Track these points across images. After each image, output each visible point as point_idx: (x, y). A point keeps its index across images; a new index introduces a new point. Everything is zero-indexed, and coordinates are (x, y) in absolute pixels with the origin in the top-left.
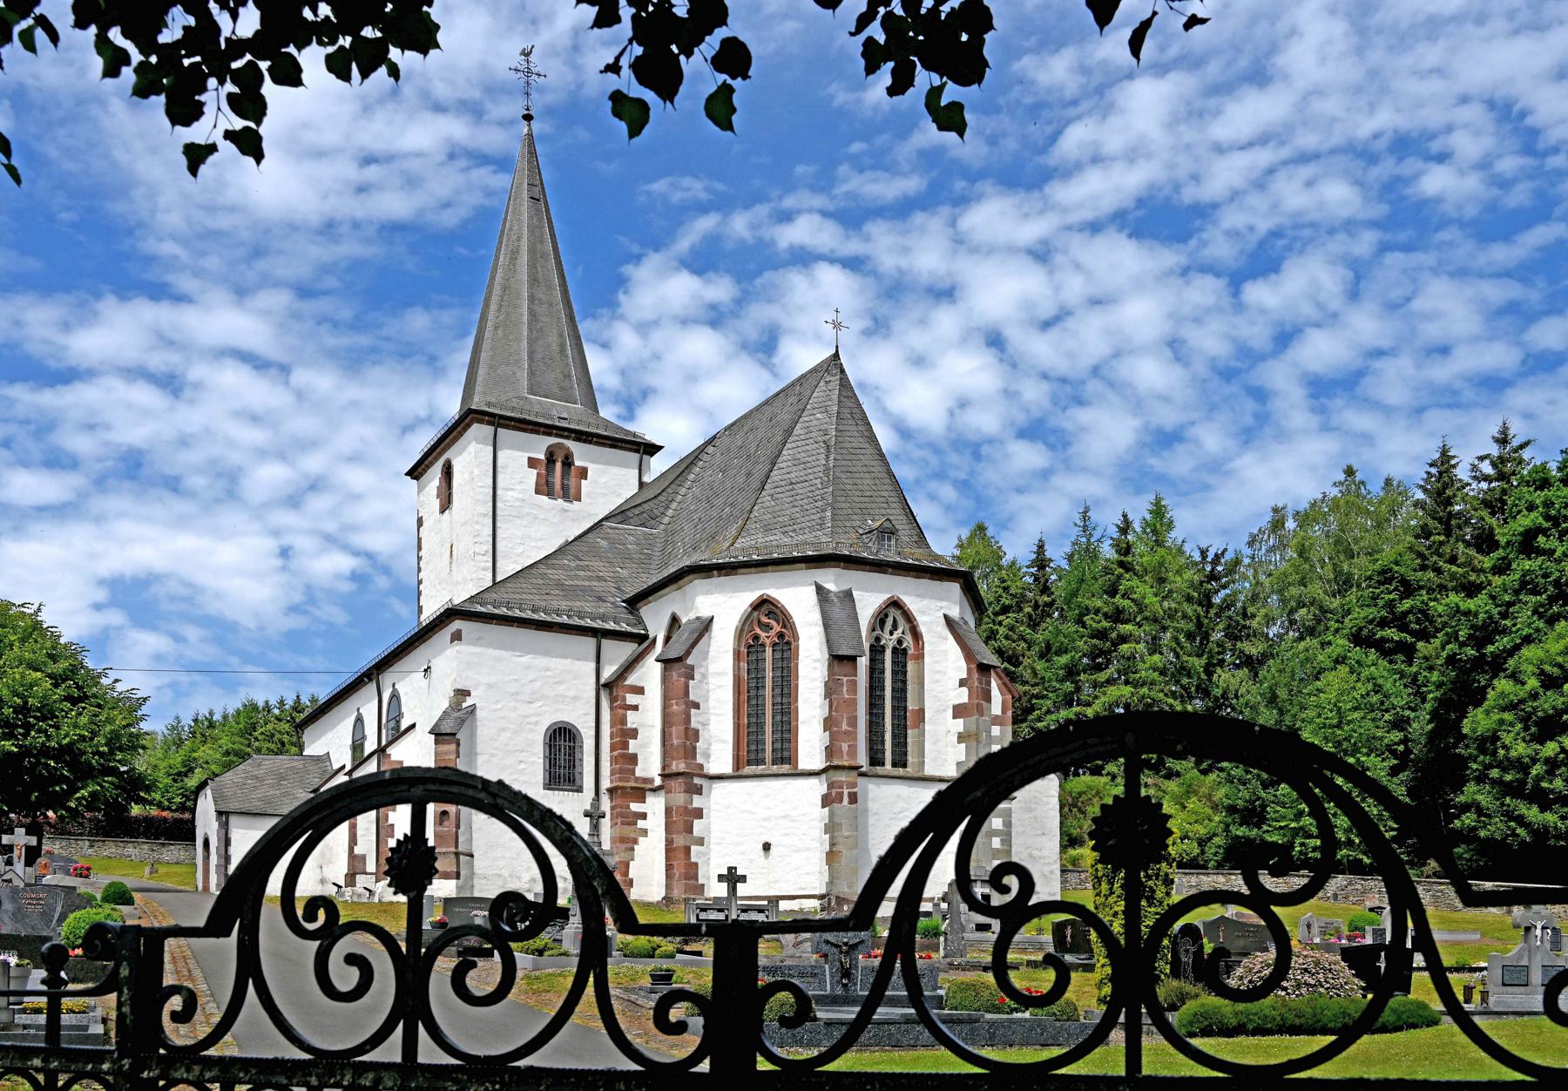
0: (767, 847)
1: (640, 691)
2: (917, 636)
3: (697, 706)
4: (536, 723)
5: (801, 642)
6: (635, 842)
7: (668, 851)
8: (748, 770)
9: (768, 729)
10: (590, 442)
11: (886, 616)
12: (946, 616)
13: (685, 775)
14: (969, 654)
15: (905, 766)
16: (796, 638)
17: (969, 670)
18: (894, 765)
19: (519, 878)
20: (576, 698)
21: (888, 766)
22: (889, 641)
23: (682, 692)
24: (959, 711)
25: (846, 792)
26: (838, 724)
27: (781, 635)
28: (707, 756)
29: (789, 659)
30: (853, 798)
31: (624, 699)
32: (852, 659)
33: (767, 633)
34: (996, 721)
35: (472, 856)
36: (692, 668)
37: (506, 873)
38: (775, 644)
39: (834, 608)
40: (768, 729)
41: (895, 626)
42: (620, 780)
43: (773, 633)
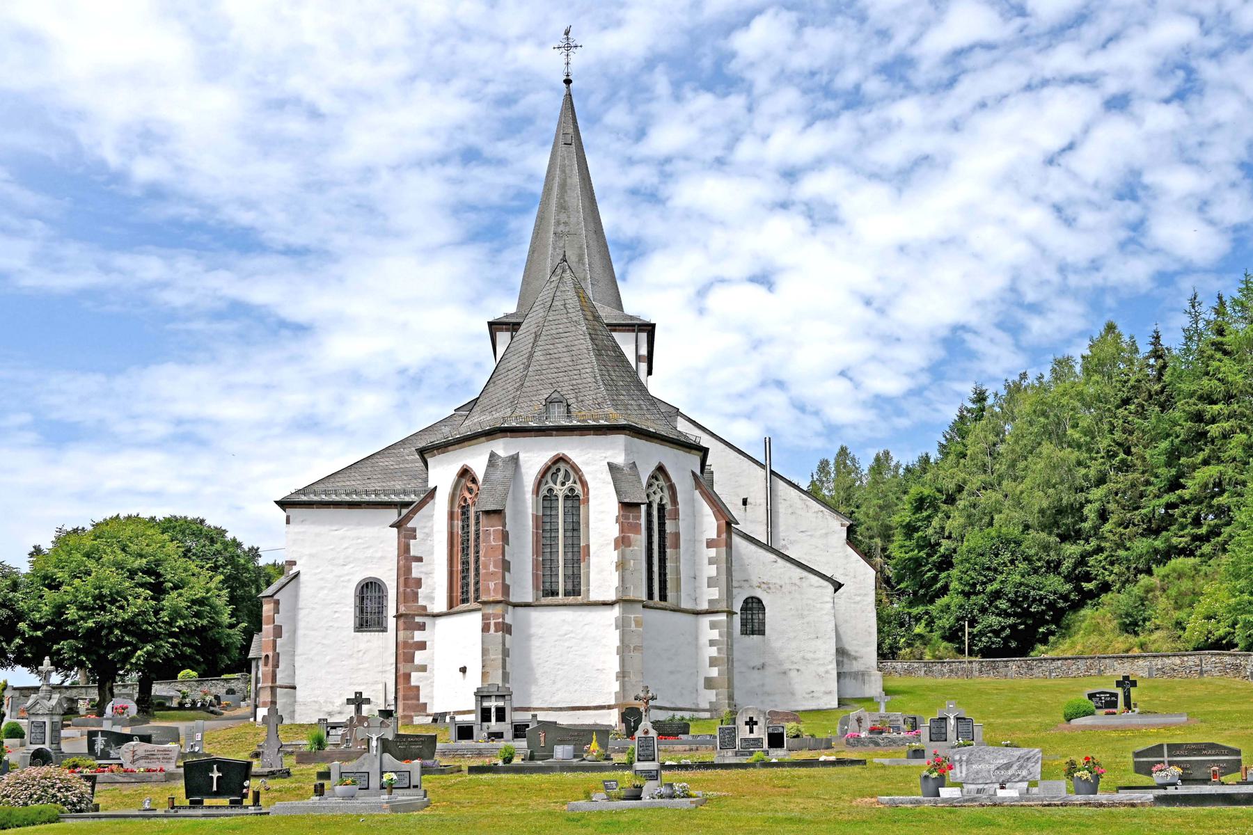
2: (584, 484)
3: (420, 559)
4: (349, 581)
11: (558, 470)
18: (566, 594)
19: (332, 703)
20: (382, 558)
22: (560, 491)
34: (710, 544)
35: (294, 688)
36: (414, 530)
37: (321, 700)
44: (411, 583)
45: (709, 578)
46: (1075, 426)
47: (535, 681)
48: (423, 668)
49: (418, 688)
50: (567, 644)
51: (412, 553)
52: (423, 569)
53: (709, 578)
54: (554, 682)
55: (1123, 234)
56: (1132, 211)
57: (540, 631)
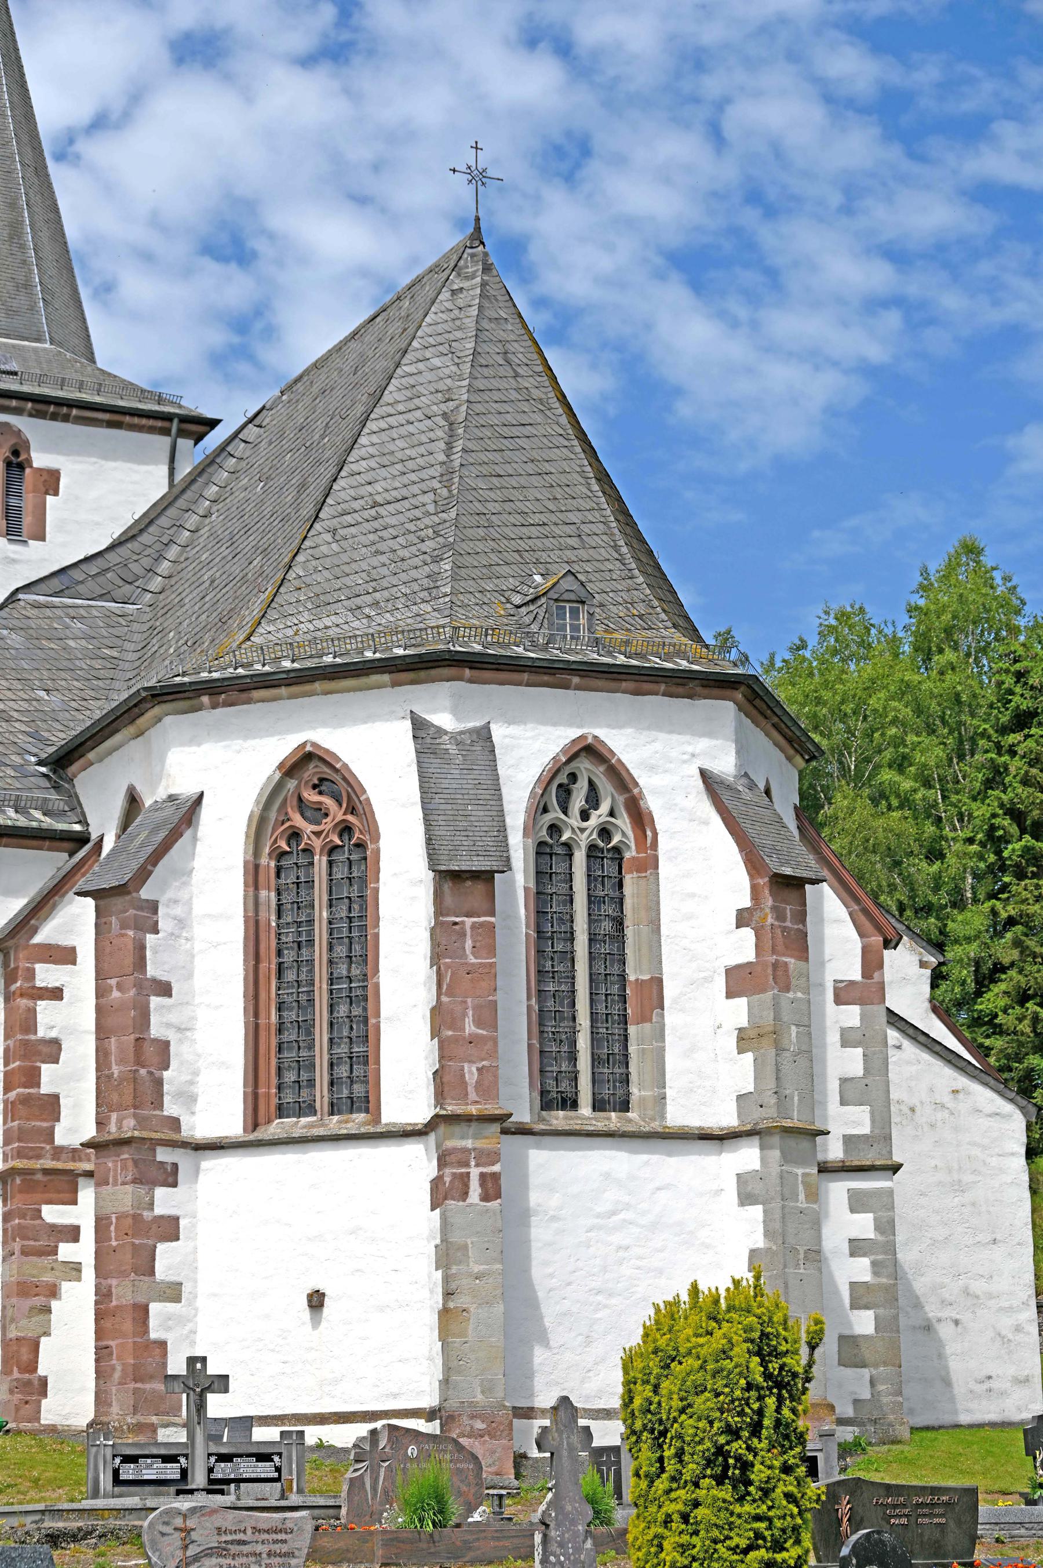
0: (316, 1301)
1: (67, 956)
2: (641, 819)
3: (165, 989)
5: (383, 843)
6: (54, 1292)
7: (100, 1316)
8: (276, 1128)
9: (322, 1035)
10: (66, 418)
11: (573, 777)
12: (704, 774)
13: (144, 1146)
14: (753, 862)
15: (624, 1106)
16: (376, 837)
17: (755, 890)
18: (598, 1105)
21: (585, 1110)
22: (580, 832)
23: (129, 960)
24: (739, 982)
25: (475, 1172)
26: (455, 1024)
27: (346, 830)
28: (190, 1099)
29: (363, 881)
30: (491, 1187)
31: (31, 974)
32: (486, 877)
33: (313, 827)
36: (153, 907)
38: (333, 849)
39: (452, 772)
40: (322, 1035)
41: (593, 799)
42: (20, 1154)
43: (327, 824)
44: (149, 1050)
45: (844, 1081)
46: (900, 764)
47: (543, 1338)
48: (173, 1293)
49: (163, 1344)
50: (617, 1238)
51: (151, 971)
52: (173, 1018)
53: (844, 1081)
54: (588, 1341)
55: (218, 337)
56: (235, 289)
57: (554, 1201)
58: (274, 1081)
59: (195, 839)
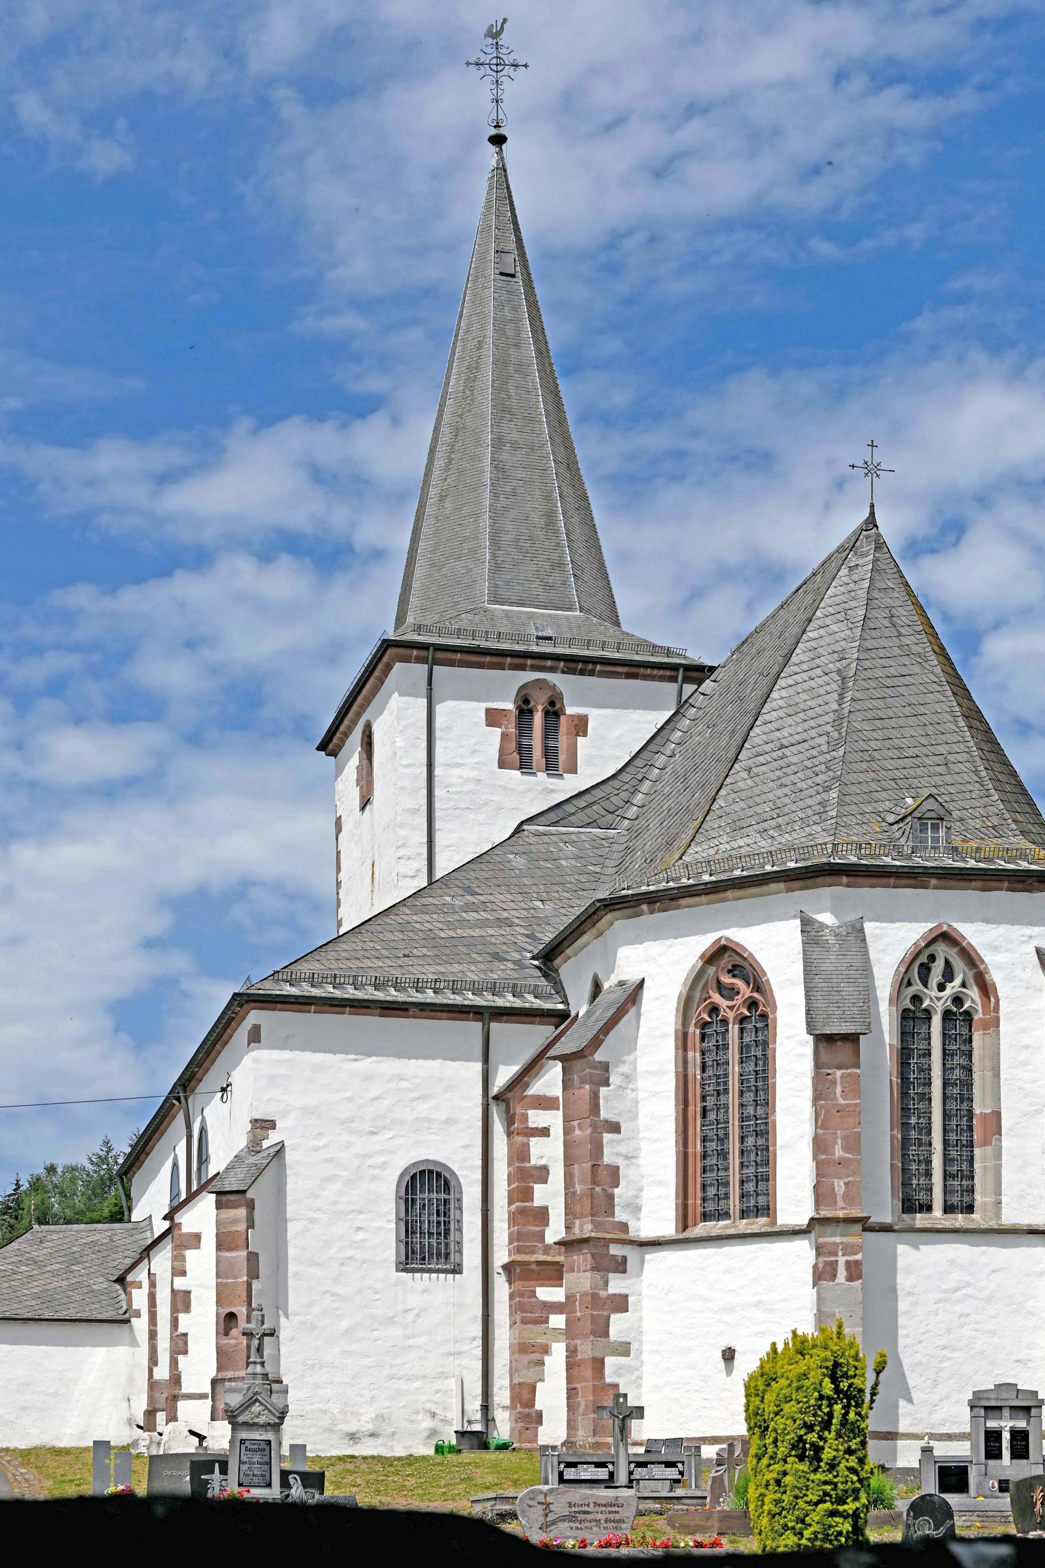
2: (986, 988)
3: (615, 1128)
11: (932, 958)
18: (948, 1209)
22: (937, 1001)
36: (605, 1067)
41: (949, 974)
44: (602, 1174)
50: (959, 1308)
51: (604, 1114)
52: (622, 1149)
54: (935, 1383)
58: (699, 1194)
59: (639, 1015)
